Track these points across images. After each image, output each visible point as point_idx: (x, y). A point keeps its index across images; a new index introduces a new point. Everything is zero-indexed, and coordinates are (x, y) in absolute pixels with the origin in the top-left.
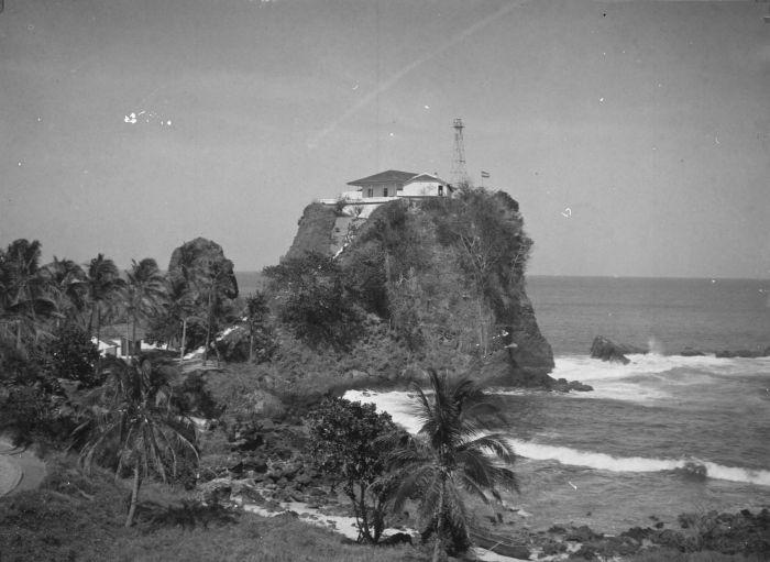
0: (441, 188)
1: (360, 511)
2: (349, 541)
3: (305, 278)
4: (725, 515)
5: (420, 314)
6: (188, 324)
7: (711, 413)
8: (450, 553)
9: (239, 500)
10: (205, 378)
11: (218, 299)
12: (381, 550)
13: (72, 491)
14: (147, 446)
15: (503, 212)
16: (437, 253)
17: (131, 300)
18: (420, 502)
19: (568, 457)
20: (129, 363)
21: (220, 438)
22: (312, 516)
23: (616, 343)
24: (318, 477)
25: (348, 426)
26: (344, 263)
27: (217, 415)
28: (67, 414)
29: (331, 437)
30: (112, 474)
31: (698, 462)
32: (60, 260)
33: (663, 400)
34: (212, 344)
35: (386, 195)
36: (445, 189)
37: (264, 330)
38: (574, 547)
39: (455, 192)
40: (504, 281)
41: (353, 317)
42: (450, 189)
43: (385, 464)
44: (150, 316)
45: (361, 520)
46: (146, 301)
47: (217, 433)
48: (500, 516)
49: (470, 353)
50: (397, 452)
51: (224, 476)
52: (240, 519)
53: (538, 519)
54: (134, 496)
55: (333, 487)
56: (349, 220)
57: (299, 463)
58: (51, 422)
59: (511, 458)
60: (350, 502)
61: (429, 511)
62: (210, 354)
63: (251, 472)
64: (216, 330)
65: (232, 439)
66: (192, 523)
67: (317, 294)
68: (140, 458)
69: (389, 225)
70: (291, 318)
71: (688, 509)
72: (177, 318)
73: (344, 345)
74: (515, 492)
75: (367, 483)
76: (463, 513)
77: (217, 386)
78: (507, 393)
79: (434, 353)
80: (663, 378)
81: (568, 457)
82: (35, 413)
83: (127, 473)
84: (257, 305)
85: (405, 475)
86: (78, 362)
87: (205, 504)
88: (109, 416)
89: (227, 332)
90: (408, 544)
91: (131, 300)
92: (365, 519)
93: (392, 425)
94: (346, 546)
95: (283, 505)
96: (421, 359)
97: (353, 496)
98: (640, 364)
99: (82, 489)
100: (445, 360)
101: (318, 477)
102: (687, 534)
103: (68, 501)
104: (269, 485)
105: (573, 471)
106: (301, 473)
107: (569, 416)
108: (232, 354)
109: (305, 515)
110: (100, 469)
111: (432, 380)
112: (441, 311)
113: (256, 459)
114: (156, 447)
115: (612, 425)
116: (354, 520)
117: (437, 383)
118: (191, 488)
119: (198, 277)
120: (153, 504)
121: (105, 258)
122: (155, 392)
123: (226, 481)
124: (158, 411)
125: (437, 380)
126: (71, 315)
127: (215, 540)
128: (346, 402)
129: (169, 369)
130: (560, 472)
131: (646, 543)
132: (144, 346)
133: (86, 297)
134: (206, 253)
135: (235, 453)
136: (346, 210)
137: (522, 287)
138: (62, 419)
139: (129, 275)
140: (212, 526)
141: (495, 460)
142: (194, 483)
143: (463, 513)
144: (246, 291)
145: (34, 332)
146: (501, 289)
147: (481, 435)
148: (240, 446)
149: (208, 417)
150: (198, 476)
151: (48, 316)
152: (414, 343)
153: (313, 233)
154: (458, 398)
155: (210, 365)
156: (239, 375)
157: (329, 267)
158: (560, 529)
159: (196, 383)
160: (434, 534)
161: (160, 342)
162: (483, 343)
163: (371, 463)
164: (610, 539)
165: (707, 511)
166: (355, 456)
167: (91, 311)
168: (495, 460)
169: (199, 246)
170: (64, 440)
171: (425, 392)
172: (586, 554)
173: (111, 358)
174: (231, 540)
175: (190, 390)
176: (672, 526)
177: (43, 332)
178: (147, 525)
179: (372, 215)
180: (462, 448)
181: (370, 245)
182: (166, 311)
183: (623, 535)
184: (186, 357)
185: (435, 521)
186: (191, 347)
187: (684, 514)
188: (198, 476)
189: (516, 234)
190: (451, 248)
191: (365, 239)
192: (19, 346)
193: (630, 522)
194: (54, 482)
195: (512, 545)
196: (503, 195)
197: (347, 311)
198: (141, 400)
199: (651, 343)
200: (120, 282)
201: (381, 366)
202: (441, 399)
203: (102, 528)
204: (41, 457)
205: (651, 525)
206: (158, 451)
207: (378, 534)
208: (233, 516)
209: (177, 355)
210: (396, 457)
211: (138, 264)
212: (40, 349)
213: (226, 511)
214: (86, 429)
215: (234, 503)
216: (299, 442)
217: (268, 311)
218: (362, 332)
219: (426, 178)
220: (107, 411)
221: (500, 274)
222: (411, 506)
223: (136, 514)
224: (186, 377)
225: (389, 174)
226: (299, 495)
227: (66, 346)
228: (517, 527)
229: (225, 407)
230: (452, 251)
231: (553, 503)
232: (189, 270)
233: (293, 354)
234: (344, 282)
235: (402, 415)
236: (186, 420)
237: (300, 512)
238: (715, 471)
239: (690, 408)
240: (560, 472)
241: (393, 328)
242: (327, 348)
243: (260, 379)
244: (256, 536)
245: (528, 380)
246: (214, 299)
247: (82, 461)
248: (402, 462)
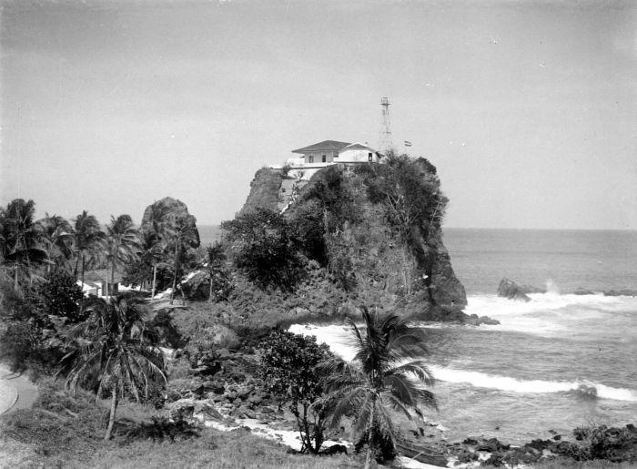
0: (370, 155)
1: (304, 426)
2: (294, 452)
3: (256, 230)
4: (613, 429)
5: (353, 261)
6: (158, 269)
7: (599, 342)
8: (379, 462)
9: (201, 417)
10: (172, 314)
11: (183, 248)
12: (321, 459)
13: (60, 410)
14: (123, 372)
15: (422, 175)
16: (368, 210)
17: (110, 249)
18: (354, 418)
19: (480, 380)
20: (108, 302)
21: (184, 365)
22: (262, 431)
23: (519, 284)
24: (268, 397)
25: (292, 354)
26: (289, 218)
27: (182, 346)
28: (56, 345)
29: (279, 364)
30: (93, 396)
31: (589, 384)
32: (51, 216)
33: (560, 332)
34: (178, 286)
35: (324, 161)
36: (374, 156)
37: (222, 274)
38: (485, 456)
39: (383, 159)
40: (425, 233)
41: (297, 263)
42: (379, 156)
43: (325, 387)
44: (126, 263)
45: (304, 434)
46: (123, 250)
47: (183, 361)
48: (422, 430)
49: (396, 293)
50: (334, 376)
51: (188, 397)
52: (202, 433)
53: (454, 432)
54: (112, 414)
55: (280, 406)
56: (293, 182)
57: (251, 386)
58: (43, 351)
59: (430, 382)
60: (294, 418)
61: (362, 426)
62: (176, 294)
63: (211, 394)
64: (181, 273)
65: (195, 366)
66: (161, 436)
67: (266, 244)
68: (117, 382)
69: (327, 186)
70: (244, 264)
71: (581, 423)
72: (149, 264)
73: (289, 286)
74: (435, 410)
75: (309, 402)
76: (391, 428)
77: (182, 321)
78: (427, 327)
79: (365, 293)
80: (559, 314)
81: (480, 380)
82: (29, 344)
83: (107, 394)
84: (215, 254)
85: (340, 396)
86: (65, 299)
87: (172, 421)
88: (92, 346)
89: (191, 275)
90: (343, 453)
91: (110, 249)
92: (307, 432)
93: (330, 354)
94: (291, 456)
95: (238, 421)
96: (354, 298)
97: (297, 414)
98: (538, 301)
99: (68, 407)
100: (375, 299)
101: (268, 397)
102: (581, 445)
103: (56, 418)
104: (227, 405)
105: (484, 392)
106: (253, 394)
107: (481, 345)
108: (196, 294)
109: (256, 430)
110: (83, 391)
111: (364, 316)
112: (371, 258)
113: (215, 383)
114: (131, 373)
115: (515, 355)
116: (298, 434)
117: (368, 318)
118: (160, 407)
119: (166, 229)
120: (128, 421)
121: (88, 214)
122: (131, 326)
123: (190, 401)
124: (134, 342)
125: (368, 315)
126: (59, 261)
127: (180, 451)
128: (290, 335)
129: (141, 306)
130: (472, 393)
131: (546, 453)
132: (121, 288)
133: (73, 248)
134: (173, 211)
135: (197, 378)
136: (291, 174)
137: (440, 237)
138: (53, 350)
139: (108, 228)
140: (178, 439)
141: (417, 383)
142: (163, 402)
143: (391, 428)
144: (207, 241)
145: (29, 276)
146: (422, 239)
147: (406, 361)
148: (202, 372)
149: (175, 347)
150: (166, 397)
151: (40, 263)
152: (348, 285)
153: (263, 193)
154: (385, 330)
155: (177, 303)
156: (199, 312)
157: (277, 221)
158: (473, 441)
159: (164, 319)
160: (366, 446)
161: (135, 285)
162: (407, 284)
163: (313, 386)
164: (515, 449)
165: (597, 426)
166: (298, 379)
167: (76, 259)
168: (417, 383)
169: (167, 204)
170: (53, 366)
171: (358, 326)
172: (495, 461)
173: (93, 298)
174: (194, 451)
175: (160, 325)
176: (569, 439)
177: (37, 276)
178: (123, 438)
179: (312, 178)
180: (390, 373)
181: (311, 203)
182: (139, 259)
183: (527, 445)
184: (156, 297)
185: (366, 435)
186: (160, 288)
187: (578, 428)
188: (166, 397)
189: (434, 194)
190: (380, 205)
191: (307, 198)
192: (16, 287)
193: (532, 435)
194: (45, 402)
195: (432, 455)
196: (423, 161)
197: (292, 258)
198: (119, 333)
199: (549, 284)
200: (101, 235)
201: (321, 304)
202: (372, 332)
203: (85, 440)
204: (34, 381)
205: (550, 437)
206: (132, 376)
207: (318, 446)
208: (196, 430)
209: (148, 295)
210: (333, 381)
211: (116, 219)
212: (34, 291)
213: (190, 427)
214: (72, 357)
215: (196, 419)
216: (251, 368)
217: (225, 258)
218: (305, 275)
219: (358, 147)
220: (90, 342)
221: (421, 227)
222: (346, 422)
223: (114, 429)
224: (156, 314)
225: (327, 143)
226: (251, 413)
227: (56, 288)
228: (436, 439)
229: (188, 339)
230: (380, 207)
231: (467, 420)
232: (159, 224)
233: (247, 294)
234: (289, 235)
235: (342, 346)
236: (156, 350)
237: (252, 427)
238: (604, 391)
239: (583, 339)
240: (472, 393)
241: (330, 272)
242: (275, 289)
243: (219, 316)
244: (215, 447)
245: (445, 316)
246: (180, 248)
247: (69, 383)
248: (339, 385)
